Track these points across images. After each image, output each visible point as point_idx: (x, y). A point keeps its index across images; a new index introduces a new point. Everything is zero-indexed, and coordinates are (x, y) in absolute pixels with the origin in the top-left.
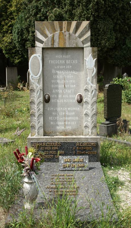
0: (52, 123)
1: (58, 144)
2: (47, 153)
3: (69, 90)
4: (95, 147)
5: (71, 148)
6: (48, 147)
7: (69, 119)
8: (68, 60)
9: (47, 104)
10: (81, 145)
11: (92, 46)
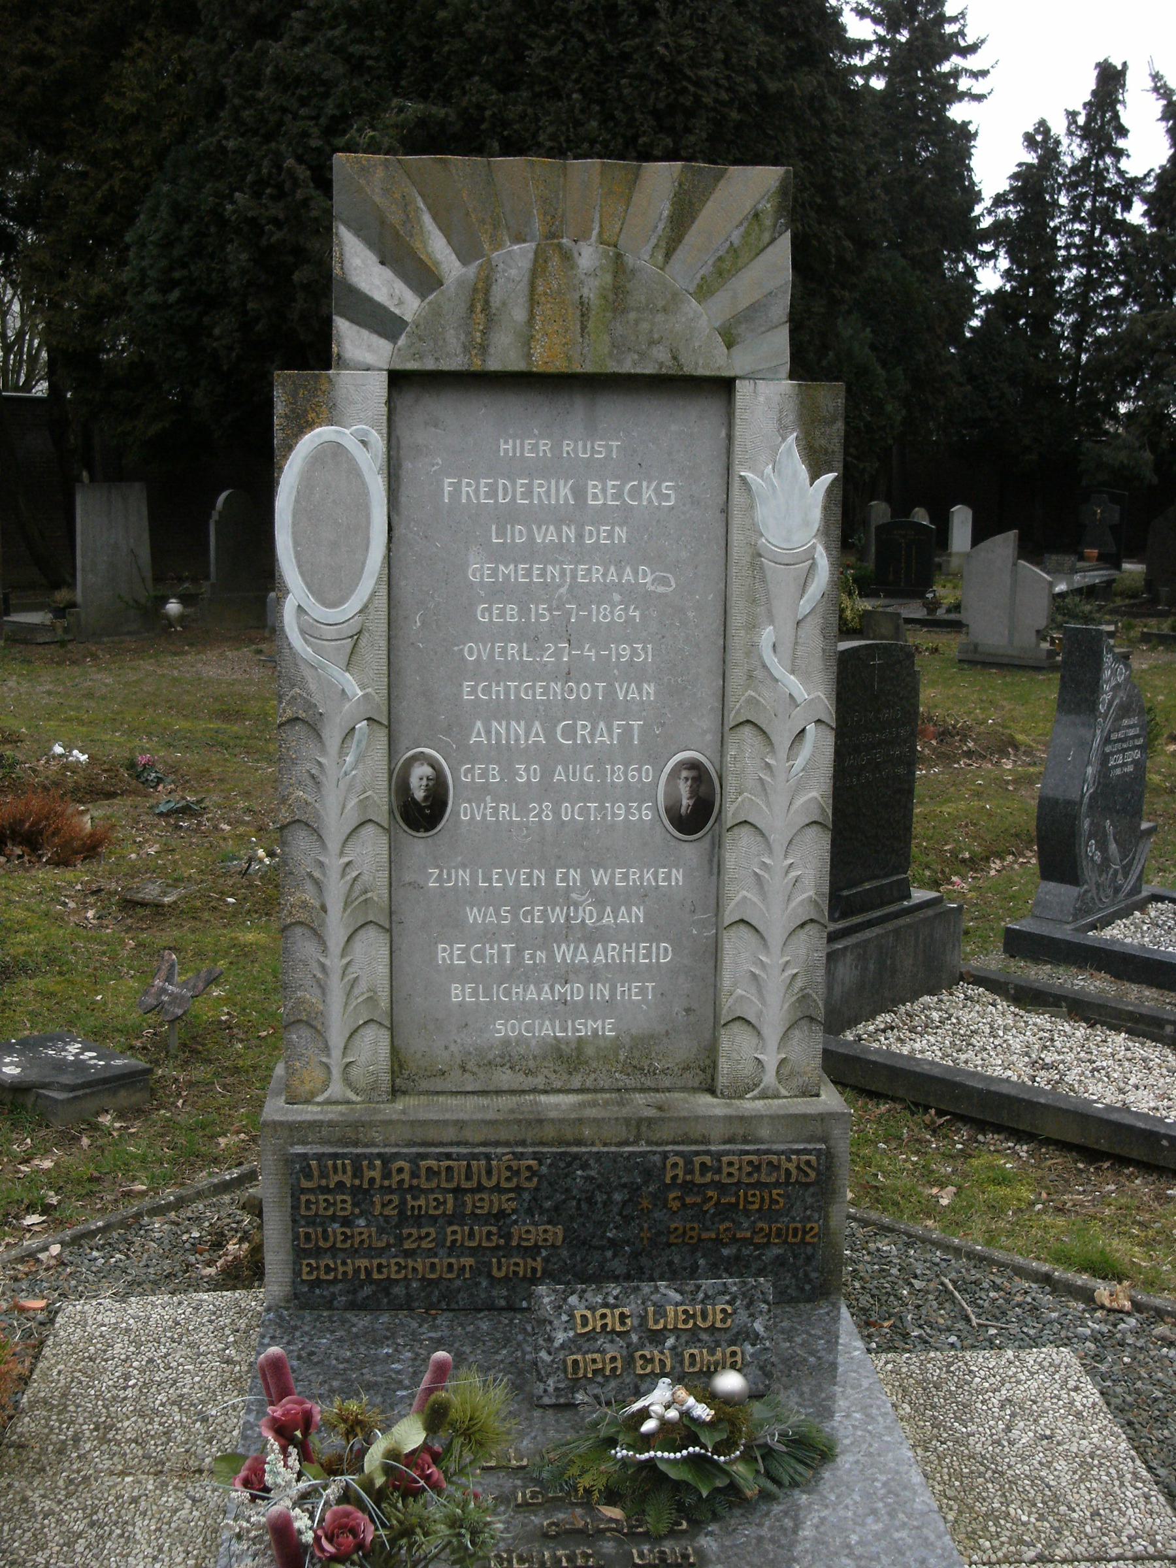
0: (458, 993)
1: (517, 1173)
2: (425, 1245)
3: (602, 725)
4: (807, 1185)
5: (617, 1197)
6: (432, 1191)
7: (599, 958)
8: (603, 481)
9: (418, 845)
10: (702, 1174)
11: (805, 365)
